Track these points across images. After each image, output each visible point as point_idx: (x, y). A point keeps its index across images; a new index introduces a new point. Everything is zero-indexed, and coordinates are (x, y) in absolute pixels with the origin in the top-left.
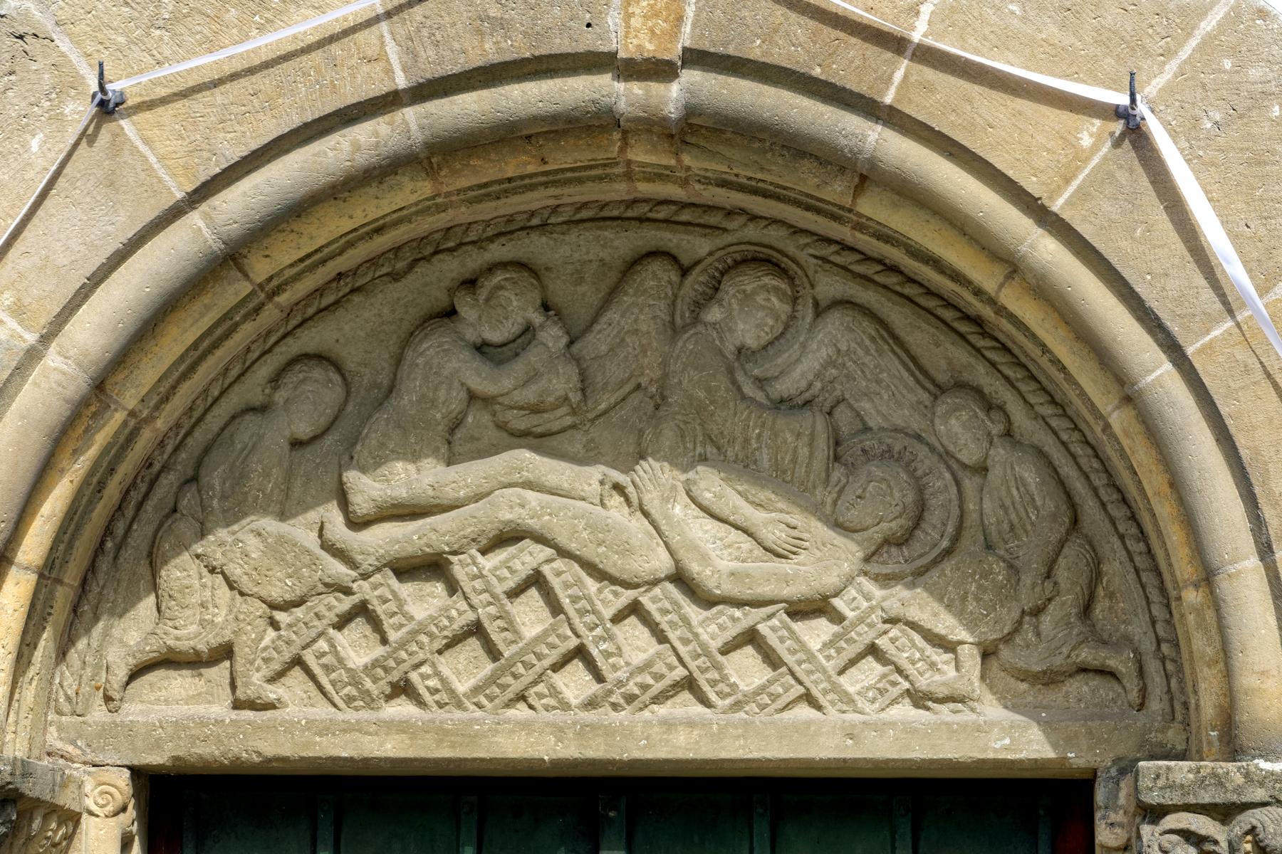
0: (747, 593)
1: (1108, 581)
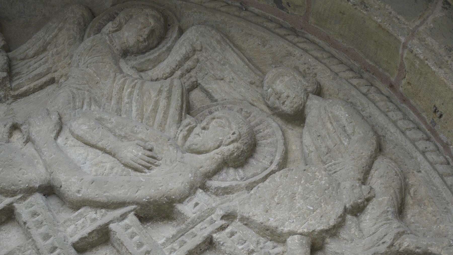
0: (102, 197)
1: (415, 191)
